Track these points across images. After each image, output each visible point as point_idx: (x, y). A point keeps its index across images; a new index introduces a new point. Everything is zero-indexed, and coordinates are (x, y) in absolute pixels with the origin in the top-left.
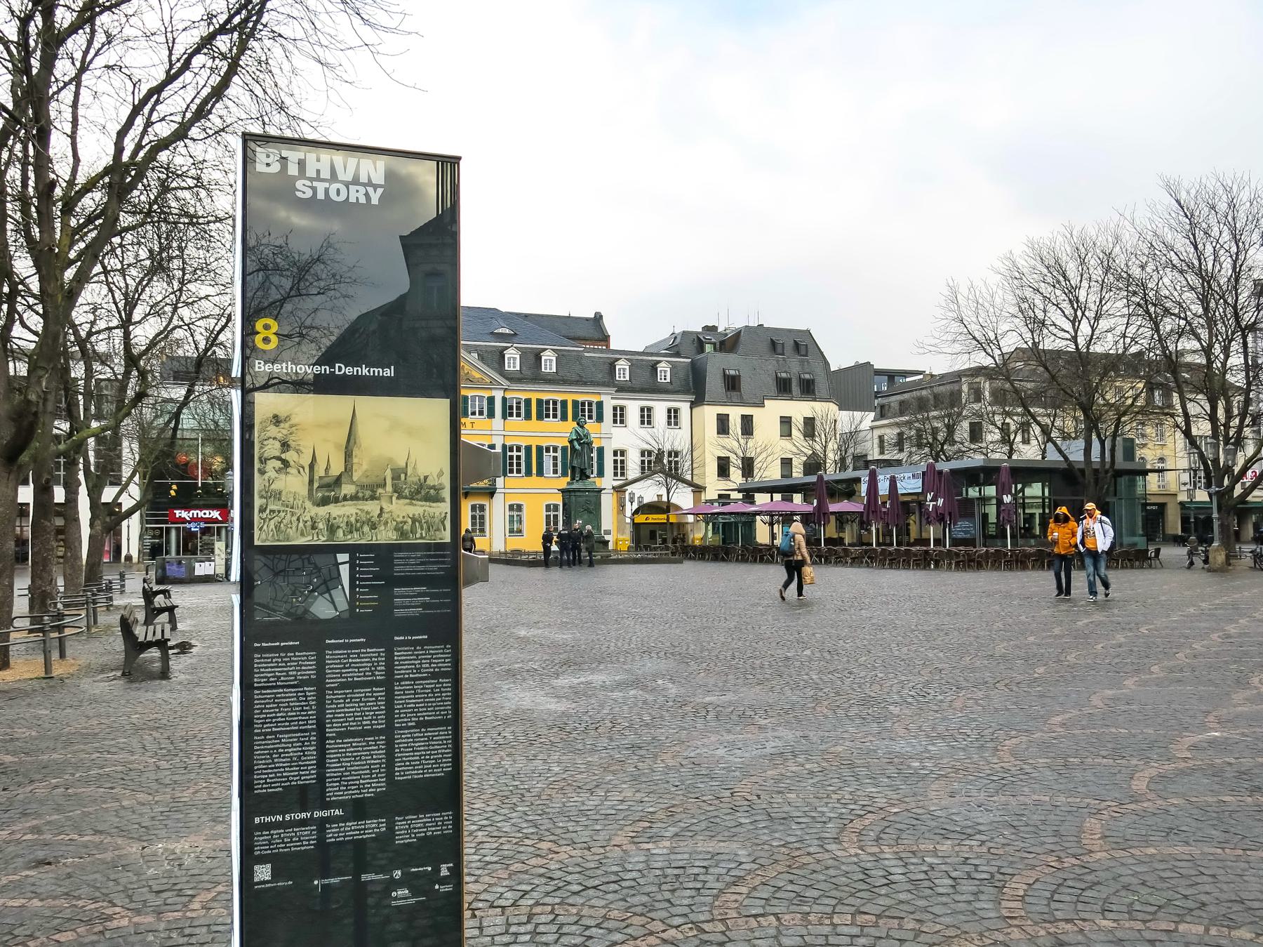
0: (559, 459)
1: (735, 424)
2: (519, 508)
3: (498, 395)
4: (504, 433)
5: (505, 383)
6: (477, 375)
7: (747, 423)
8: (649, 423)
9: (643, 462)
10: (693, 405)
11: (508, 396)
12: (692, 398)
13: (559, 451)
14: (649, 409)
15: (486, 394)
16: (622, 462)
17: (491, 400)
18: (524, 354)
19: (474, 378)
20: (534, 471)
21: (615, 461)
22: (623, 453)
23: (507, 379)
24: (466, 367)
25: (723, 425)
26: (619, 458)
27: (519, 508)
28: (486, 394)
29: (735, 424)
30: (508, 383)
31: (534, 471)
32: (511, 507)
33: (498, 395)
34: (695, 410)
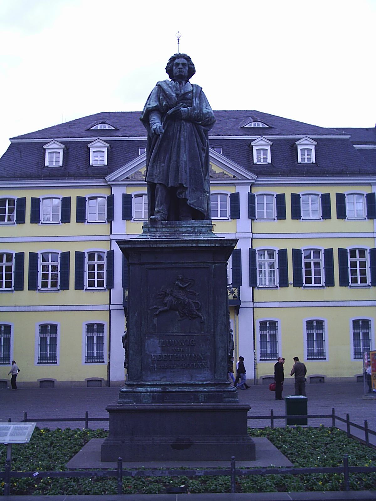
0: (322, 265)
2: (273, 325)
3: (244, 192)
4: (250, 235)
5: (251, 177)
11: (257, 191)
13: (322, 256)
15: (230, 190)
17: (235, 198)
18: (276, 146)
19: (214, 173)
20: (291, 279)
27: (273, 325)
28: (230, 190)
30: (255, 177)
31: (291, 279)
32: (263, 325)
33: (244, 192)
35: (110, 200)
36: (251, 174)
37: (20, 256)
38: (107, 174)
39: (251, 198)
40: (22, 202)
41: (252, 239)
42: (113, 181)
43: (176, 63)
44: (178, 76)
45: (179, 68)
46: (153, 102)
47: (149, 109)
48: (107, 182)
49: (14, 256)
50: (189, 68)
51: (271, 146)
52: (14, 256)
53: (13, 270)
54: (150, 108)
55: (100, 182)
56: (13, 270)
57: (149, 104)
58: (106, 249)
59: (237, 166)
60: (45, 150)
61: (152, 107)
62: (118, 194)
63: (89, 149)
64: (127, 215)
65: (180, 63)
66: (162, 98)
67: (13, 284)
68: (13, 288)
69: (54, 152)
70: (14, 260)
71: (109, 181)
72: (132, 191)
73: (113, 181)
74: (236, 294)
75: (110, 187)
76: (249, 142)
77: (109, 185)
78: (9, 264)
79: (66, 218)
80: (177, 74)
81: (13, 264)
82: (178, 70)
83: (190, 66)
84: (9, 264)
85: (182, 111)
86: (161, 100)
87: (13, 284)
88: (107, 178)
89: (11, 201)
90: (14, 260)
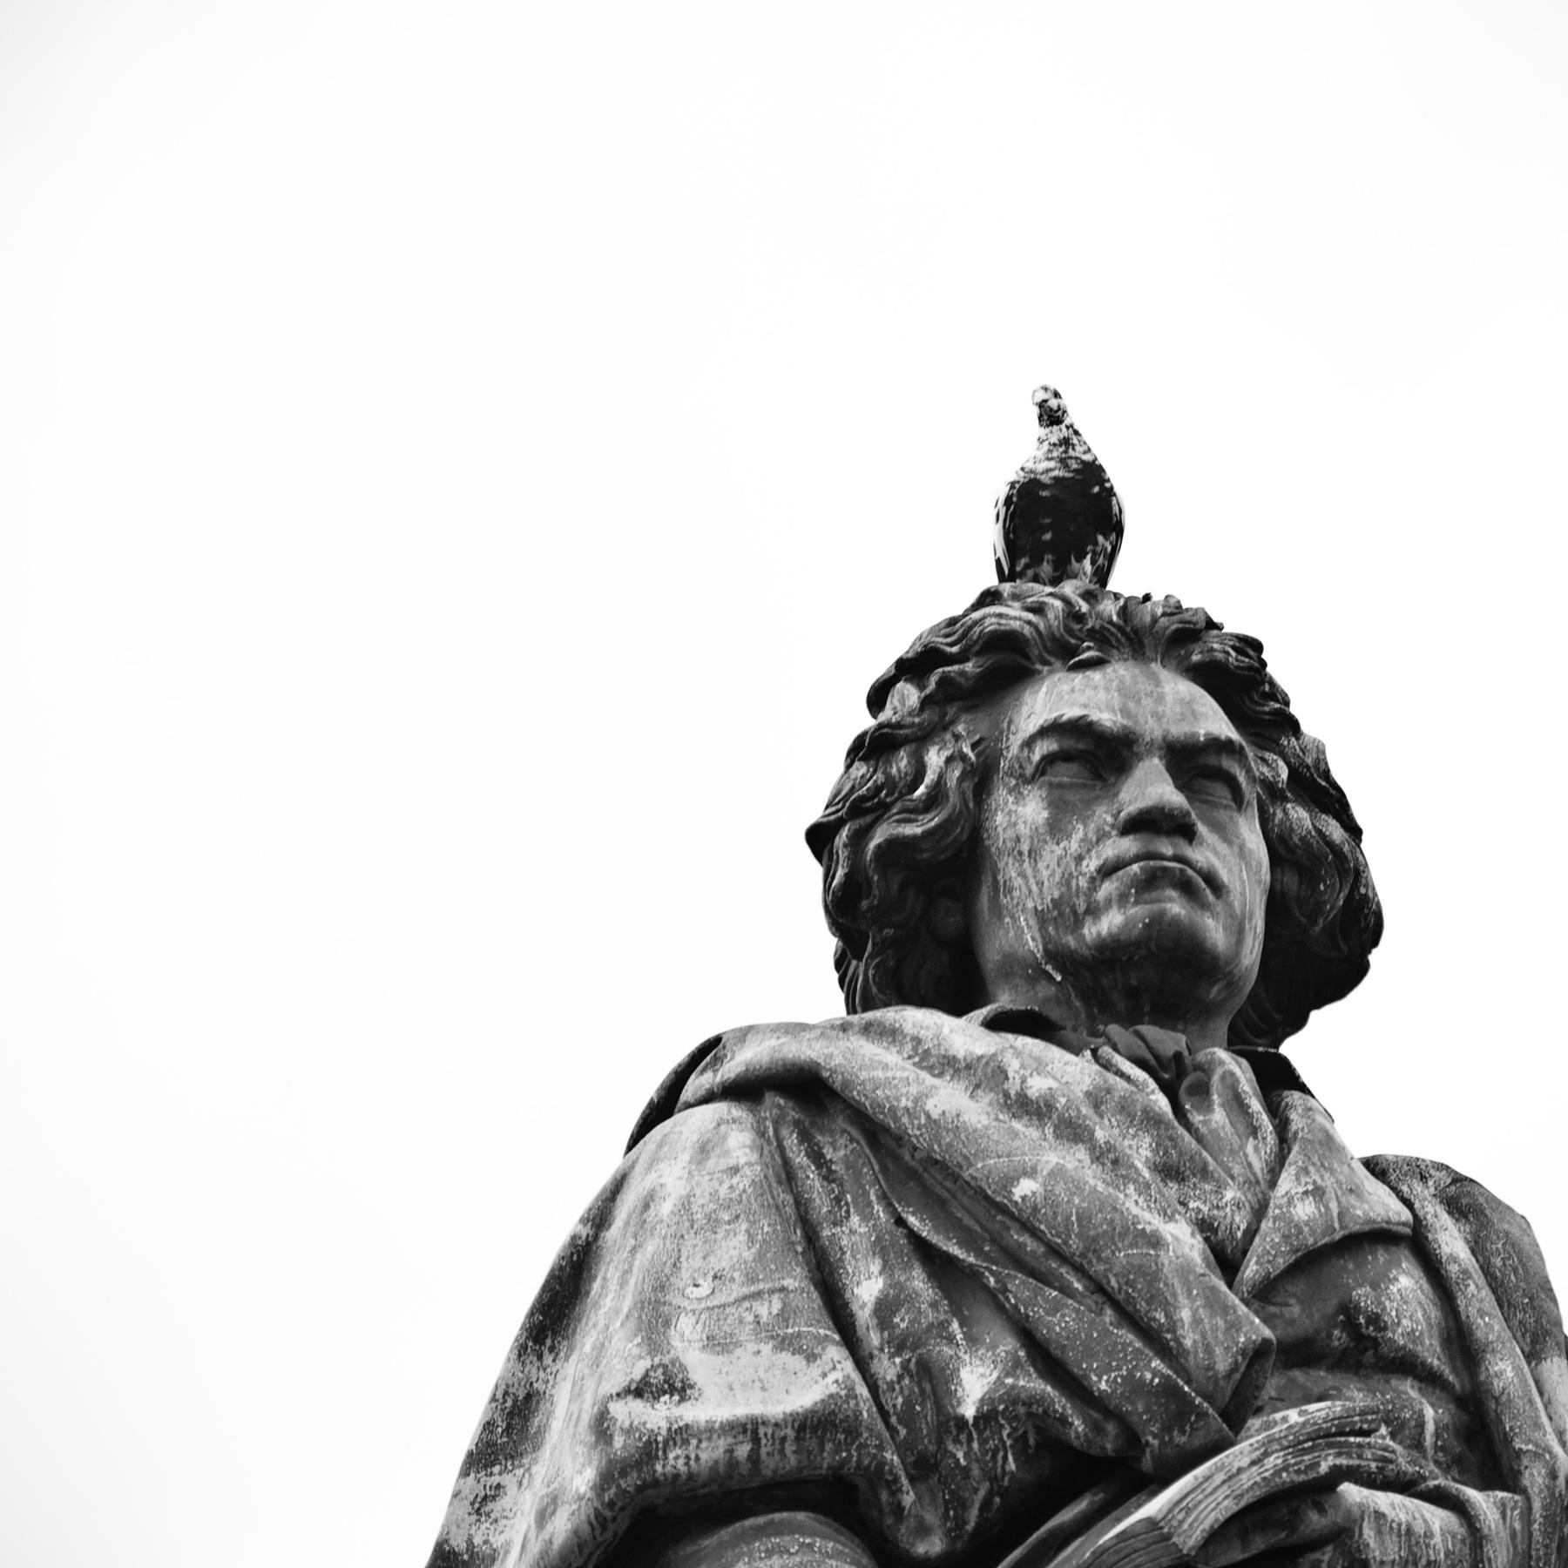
43: (1053, 729)
44: (1112, 952)
45: (1146, 823)
46: (718, 1344)
47: (674, 1460)
50: (1280, 846)
54: (710, 1453)
57: (673, 1385)
61: (750, 1429)
65: (1151, 729)
66: (885, 1309)
80: (1110, 923)
82: (1128, 845)
83: (1299, 816)
85: (1369, 1533)
86: (875, 1339)
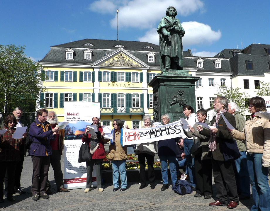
1: (252, 84)
3: (145, 72)
5: (148, 67)
6: (135, 63)
7: (257, 83)
8: (213, 85)
9: (210, 102)
10: (232, 77)
12: (231, 74)
14: (213, 79)
16: (201, 102)
17: (142, 74)
21: (198, 102)
22: (201, 98)
23: (149, 65)
24: (130, 60)
25: (246, 84)
26: (200, 101)
28: (139, 72)
29: (252, 84)
30: (149, 67)
34: (232, 80)
35: (93, 73)
36: (148, 66)
37: (56, 95)
38: (92, 63)
39: (148, 74)
40: (56, 73)
41: (148, 90)
42: (94, 66)
48: (92, 66)
49: (53, 94)
51: (155, 55)
52: (53, 94)
53: (53, 99)
55: (89, 66)
56: (53, 99)
58: (92, 93)
59: (142, 62)
60: (65, 52)
62: (96, 71)
63: (84, 53)
64: (100, 80)
67: (53, 105)
68: (53, 107)
69: (69, 53)
70: (53, 96)
71: (93, 66)
72: (102, 71)
73: (94, 66)
74: (142, 110)
75: (93, 68)
76: (146, 54)
77: (92, 67)
78: (51, 97)
79: (75, 80)
81: (53, 97)
84: (51, 97)
87: (53, 105)
88: (92, 64)
89: (52, 72)
90: (53, 96)
